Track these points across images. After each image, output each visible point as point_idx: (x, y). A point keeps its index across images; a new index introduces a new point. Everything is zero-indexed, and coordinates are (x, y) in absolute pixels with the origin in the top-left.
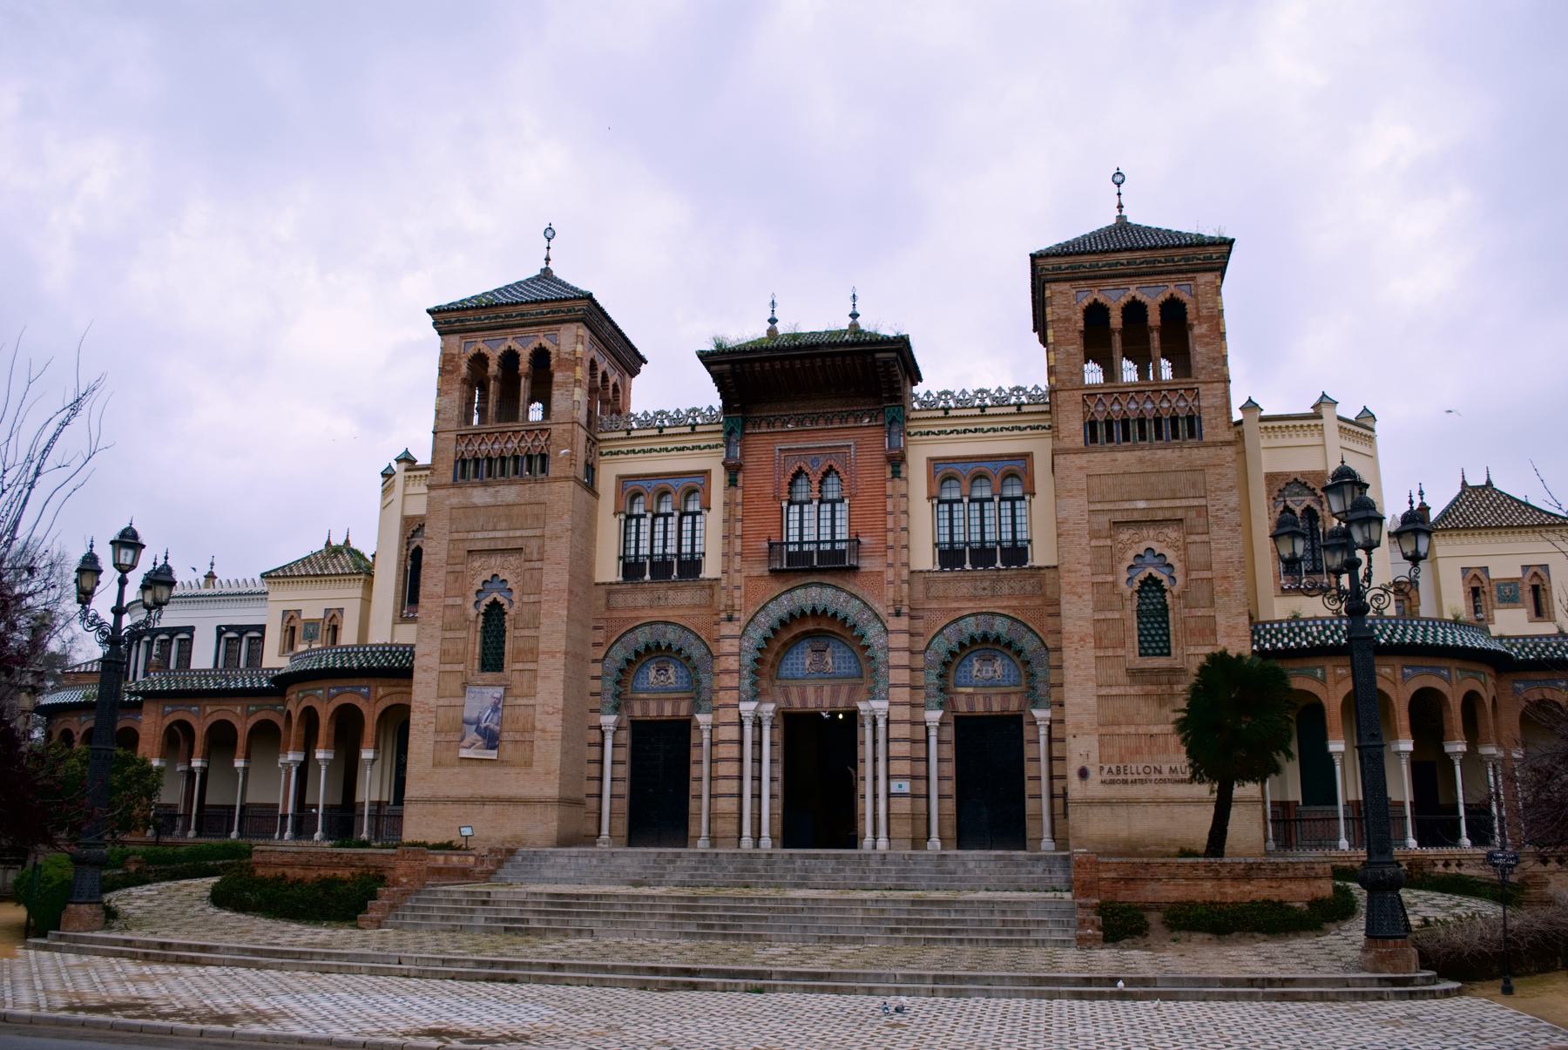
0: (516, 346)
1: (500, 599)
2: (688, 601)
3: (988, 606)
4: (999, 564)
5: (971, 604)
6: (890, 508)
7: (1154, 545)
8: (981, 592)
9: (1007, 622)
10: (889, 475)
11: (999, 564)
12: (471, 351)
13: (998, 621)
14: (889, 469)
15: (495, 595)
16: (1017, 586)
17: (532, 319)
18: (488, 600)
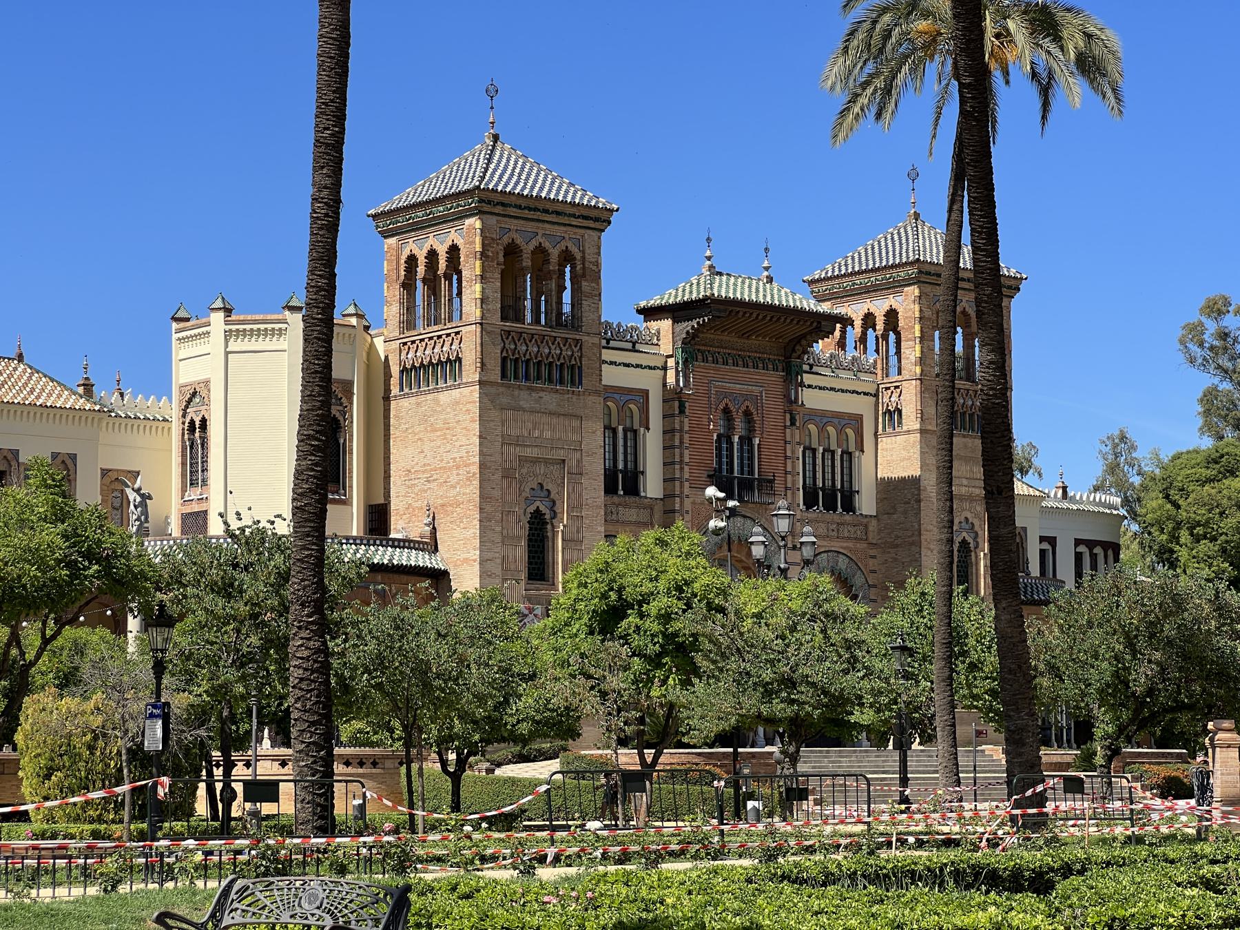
0: (547, 245)
1: (542, 508)
2: (633, 519)
3: (836, 545)
4: (840, 510)
5: (825, 543)
6: (789, 454)
7: (969, 515)
8: (831, 533)
9: (847, 560)
10: (788, 423)
11: (840, 510)
12: (506, 240)
13: (841, 558)
14: (788, 416)
15: (538, 503)
16: (852, 529)
17: (565, 220)
18: (532, 509)
